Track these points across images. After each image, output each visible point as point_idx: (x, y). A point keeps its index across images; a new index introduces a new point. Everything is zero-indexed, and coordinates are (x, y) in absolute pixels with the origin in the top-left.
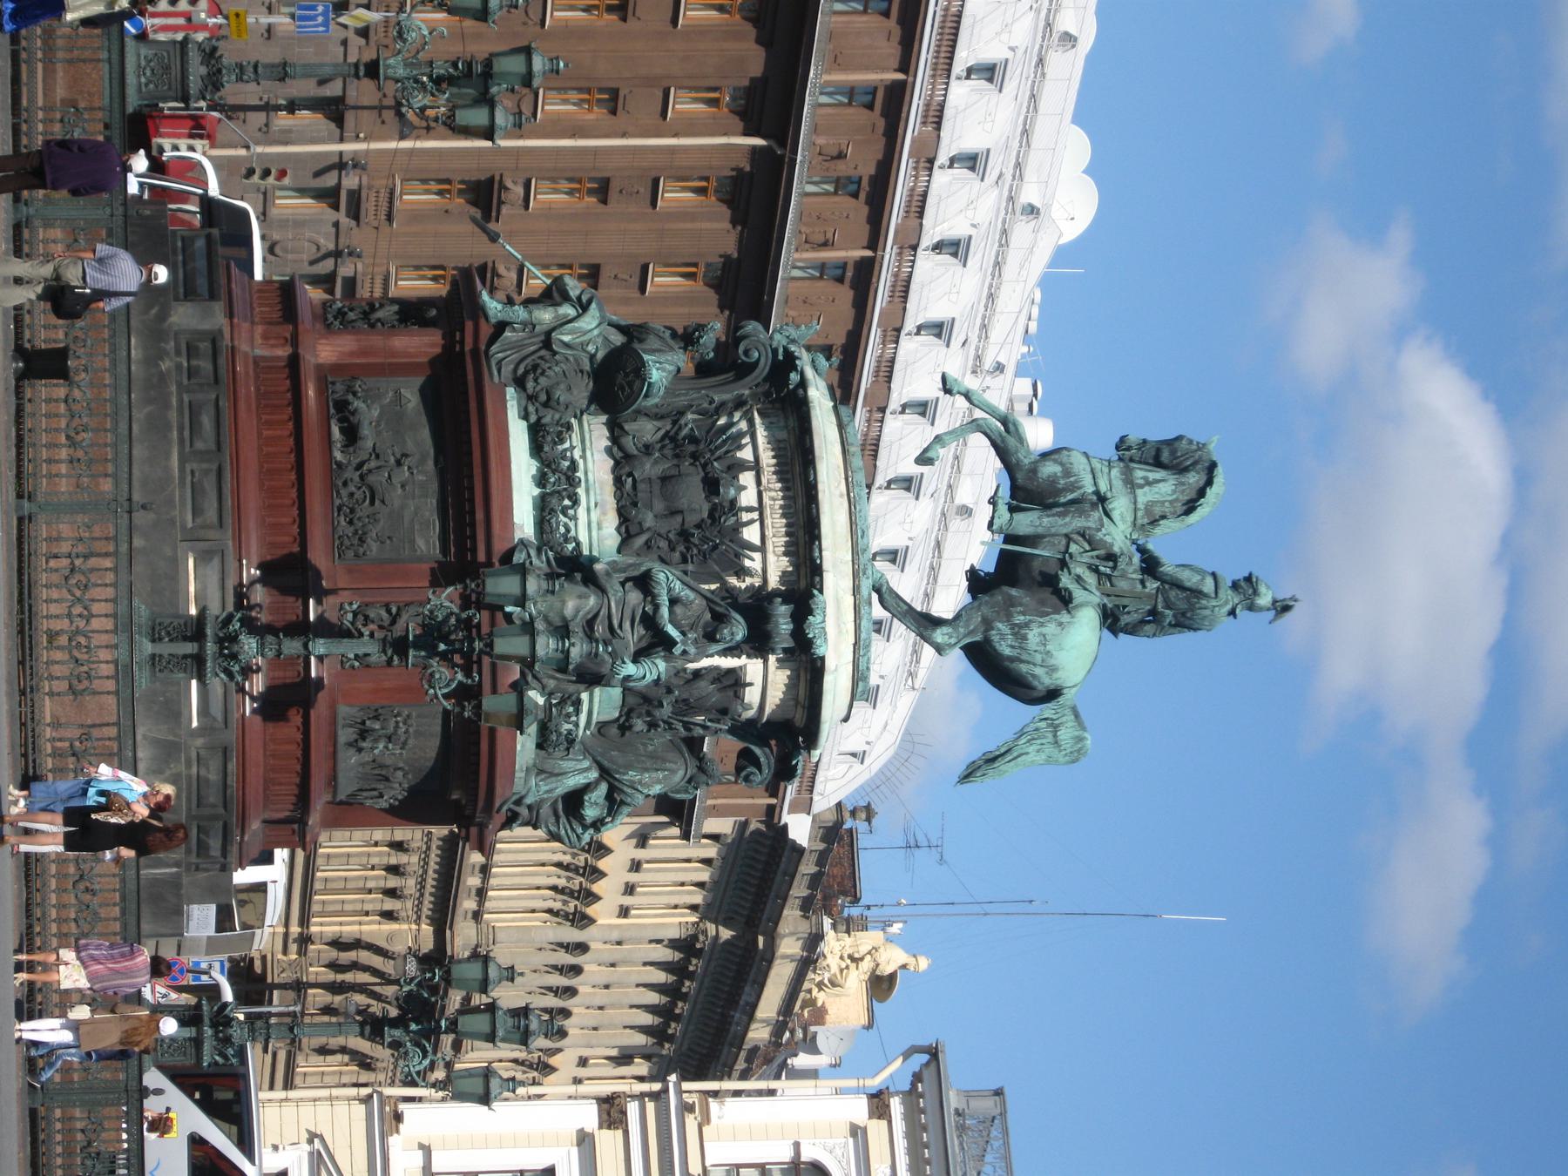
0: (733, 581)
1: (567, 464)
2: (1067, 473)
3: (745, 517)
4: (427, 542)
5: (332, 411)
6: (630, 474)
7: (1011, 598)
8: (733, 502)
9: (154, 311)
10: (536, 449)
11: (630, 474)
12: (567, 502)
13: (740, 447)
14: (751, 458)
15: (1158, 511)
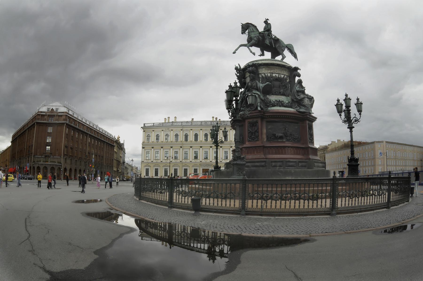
0: (288, 81)
1: (276, 102)
2: (256, 37)
6: (275, 92)
7: (278, 46)
11: (275, 92)
12: (283, 102)
13: (268, 75)
14: (270, 74)
15: (256, 30)
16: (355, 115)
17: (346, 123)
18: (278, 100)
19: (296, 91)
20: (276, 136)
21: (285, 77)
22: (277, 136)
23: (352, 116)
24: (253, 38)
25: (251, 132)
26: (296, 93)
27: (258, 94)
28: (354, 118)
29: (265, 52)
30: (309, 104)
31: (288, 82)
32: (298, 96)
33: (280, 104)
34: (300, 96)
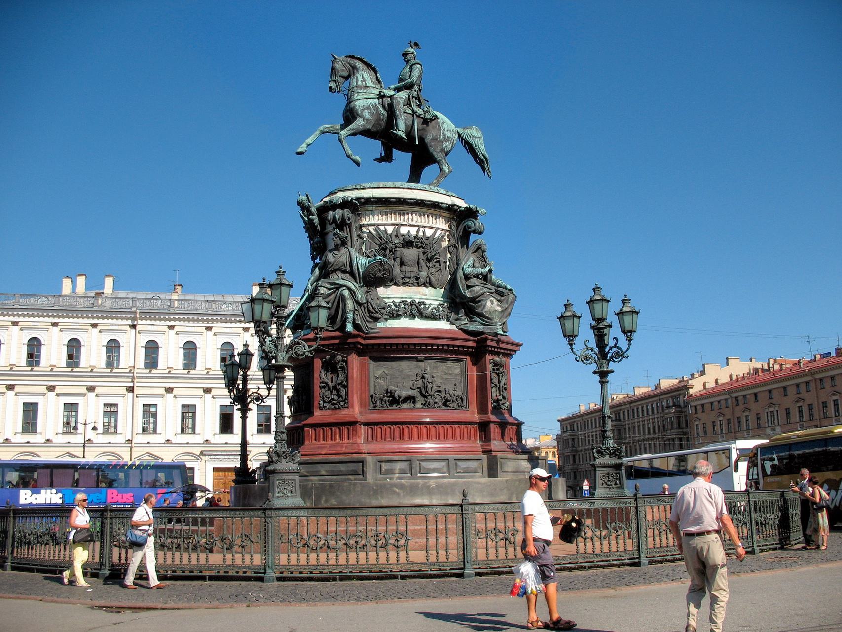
1: (402, 305)
2: (368, 108)
3: (421, 233)
4: (455, 368)
6: (402, 279)
7: (432, 139)
8: (415, 238)
9: (397, 490)
10: (398, 316)
12: (422, 306)
13: (386, 231)
15: (375, 81)
16: (615, 341)
17: (588, 362)
18: (409, 300)
19: (463, 276)
20: (396, 396)
21: (436, 235)
22: (400, 398)
24: (359, 111)
25: (328, 385)
26: (464, 282)
27: (349, 289)
28: (614, 349)
29: (395, 152)
30: (495, 310)
31: (445, 248)
32: (468, 287)
33: (417, 310)
34: (474, 288)
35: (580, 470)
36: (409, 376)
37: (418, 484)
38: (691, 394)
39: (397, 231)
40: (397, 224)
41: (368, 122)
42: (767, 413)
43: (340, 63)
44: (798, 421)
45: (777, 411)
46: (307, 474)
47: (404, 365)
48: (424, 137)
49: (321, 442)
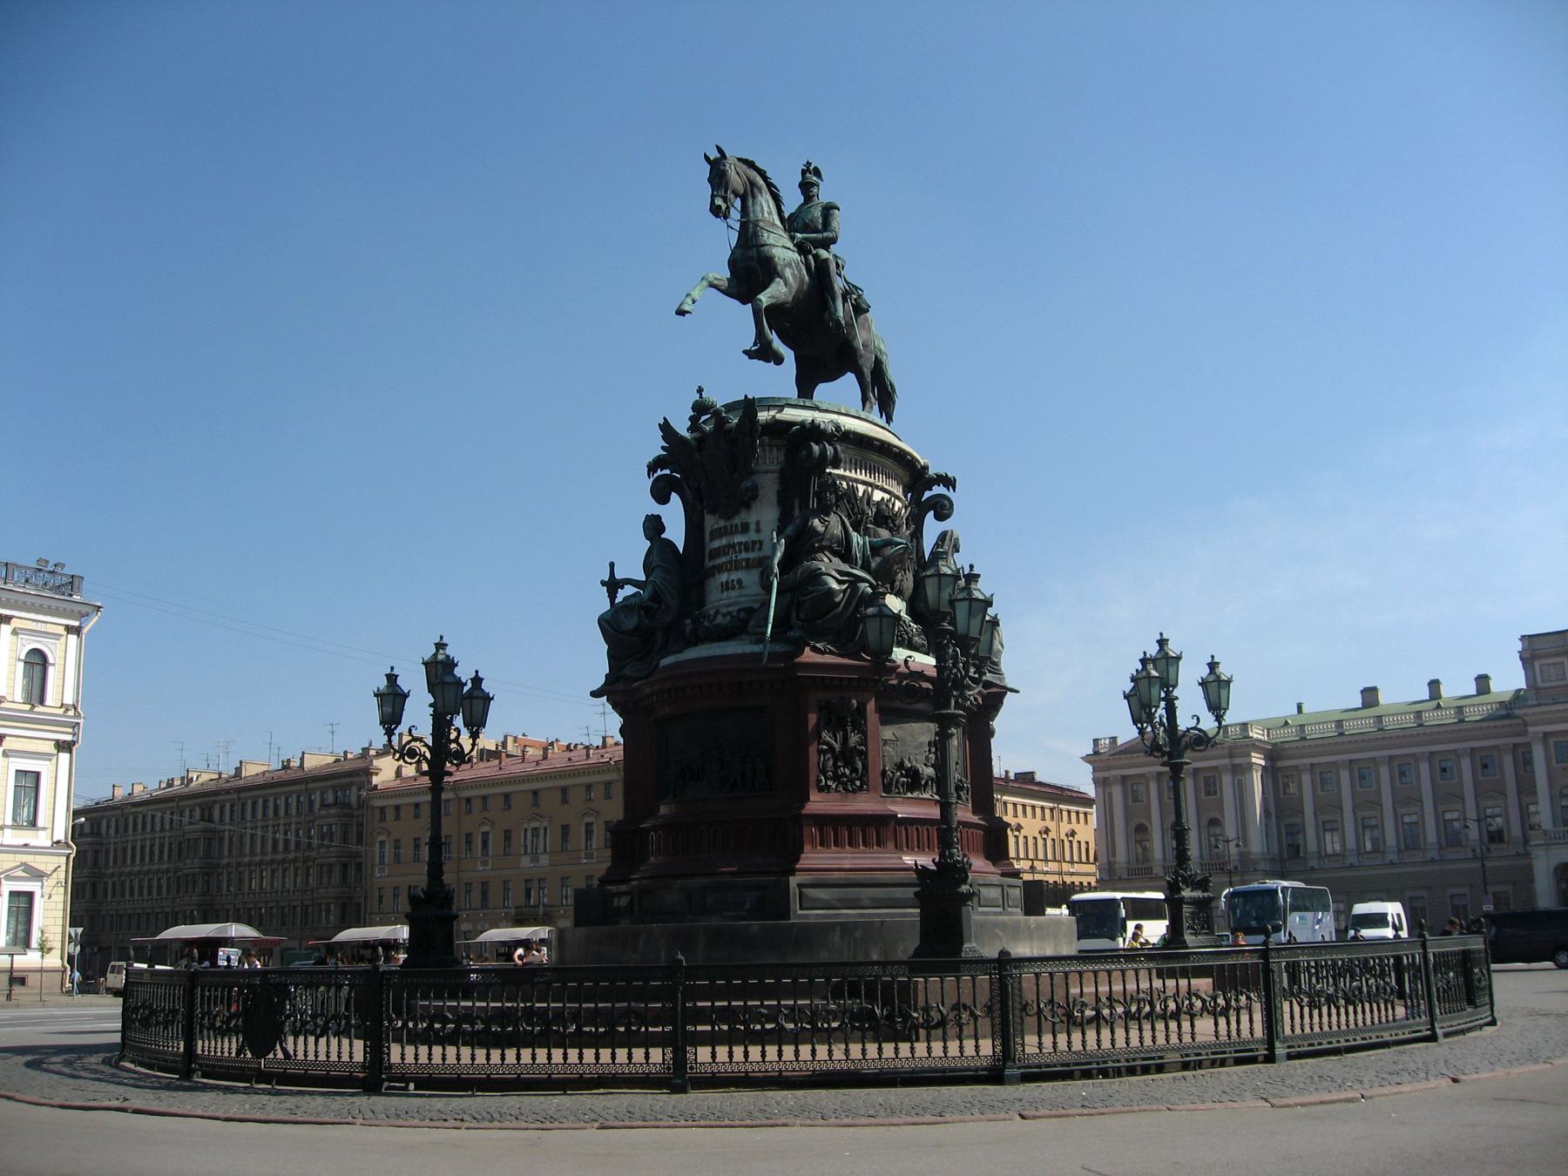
2: (789, 265)
5: (915, 795)
9: (1000, 933)
23: (1184, 723)
24: (779, 267)
25: (831, 748)
35: (104, 913)
36: (921, 745)
37: (1019, 922)
38: (376, 786)
39: (870, 497)
40: (870, 485)
41: (790, 291)
42: (526, 830)
43: (733, 167)
44: (583, 847)
45: (545, 828)
46: (840, 906)
47: (916, 726)
48: (850, 338)
49: (833, 847)
